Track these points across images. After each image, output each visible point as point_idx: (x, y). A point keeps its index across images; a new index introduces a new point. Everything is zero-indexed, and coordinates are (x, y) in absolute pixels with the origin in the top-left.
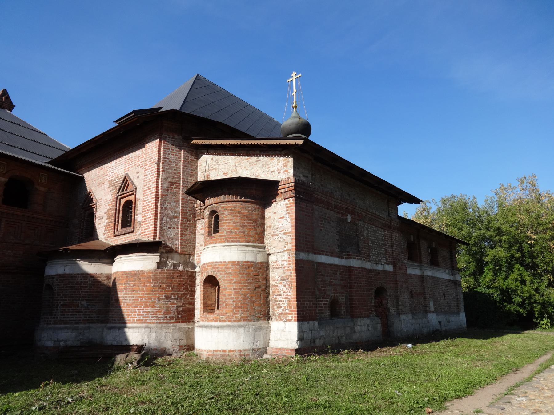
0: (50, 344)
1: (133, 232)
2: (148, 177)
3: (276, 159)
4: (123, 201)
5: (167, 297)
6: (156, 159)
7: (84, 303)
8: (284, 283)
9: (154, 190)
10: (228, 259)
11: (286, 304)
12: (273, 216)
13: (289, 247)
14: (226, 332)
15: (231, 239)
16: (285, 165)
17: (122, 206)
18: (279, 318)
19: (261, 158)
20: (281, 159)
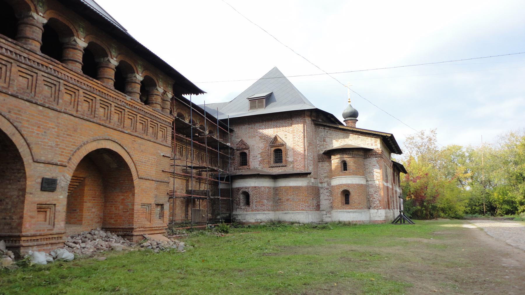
0: (253, 221)
1: (286, 166)
2: (296, 139)
3: (370, 138)
4: (273, 149)
5: (313, 199)
6: (302, 131)
7: (265, 201)
8: (376, 193)
9: (302, 146)
10: (354, 183)
11: (378, 202)
12: (369, 164)
13: (379, 178)
14: (357, 214)
15: (355, 174)
16: (376, 142)
17: (272, 152)
18: (374, 208)
19: (360, 136)
20: (373, 139)
